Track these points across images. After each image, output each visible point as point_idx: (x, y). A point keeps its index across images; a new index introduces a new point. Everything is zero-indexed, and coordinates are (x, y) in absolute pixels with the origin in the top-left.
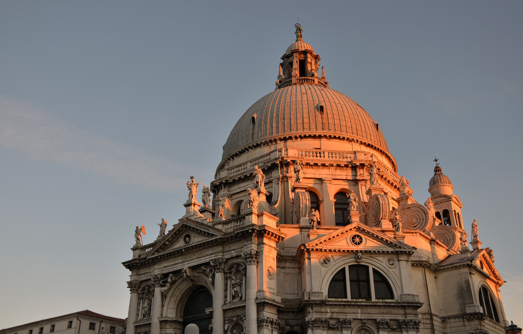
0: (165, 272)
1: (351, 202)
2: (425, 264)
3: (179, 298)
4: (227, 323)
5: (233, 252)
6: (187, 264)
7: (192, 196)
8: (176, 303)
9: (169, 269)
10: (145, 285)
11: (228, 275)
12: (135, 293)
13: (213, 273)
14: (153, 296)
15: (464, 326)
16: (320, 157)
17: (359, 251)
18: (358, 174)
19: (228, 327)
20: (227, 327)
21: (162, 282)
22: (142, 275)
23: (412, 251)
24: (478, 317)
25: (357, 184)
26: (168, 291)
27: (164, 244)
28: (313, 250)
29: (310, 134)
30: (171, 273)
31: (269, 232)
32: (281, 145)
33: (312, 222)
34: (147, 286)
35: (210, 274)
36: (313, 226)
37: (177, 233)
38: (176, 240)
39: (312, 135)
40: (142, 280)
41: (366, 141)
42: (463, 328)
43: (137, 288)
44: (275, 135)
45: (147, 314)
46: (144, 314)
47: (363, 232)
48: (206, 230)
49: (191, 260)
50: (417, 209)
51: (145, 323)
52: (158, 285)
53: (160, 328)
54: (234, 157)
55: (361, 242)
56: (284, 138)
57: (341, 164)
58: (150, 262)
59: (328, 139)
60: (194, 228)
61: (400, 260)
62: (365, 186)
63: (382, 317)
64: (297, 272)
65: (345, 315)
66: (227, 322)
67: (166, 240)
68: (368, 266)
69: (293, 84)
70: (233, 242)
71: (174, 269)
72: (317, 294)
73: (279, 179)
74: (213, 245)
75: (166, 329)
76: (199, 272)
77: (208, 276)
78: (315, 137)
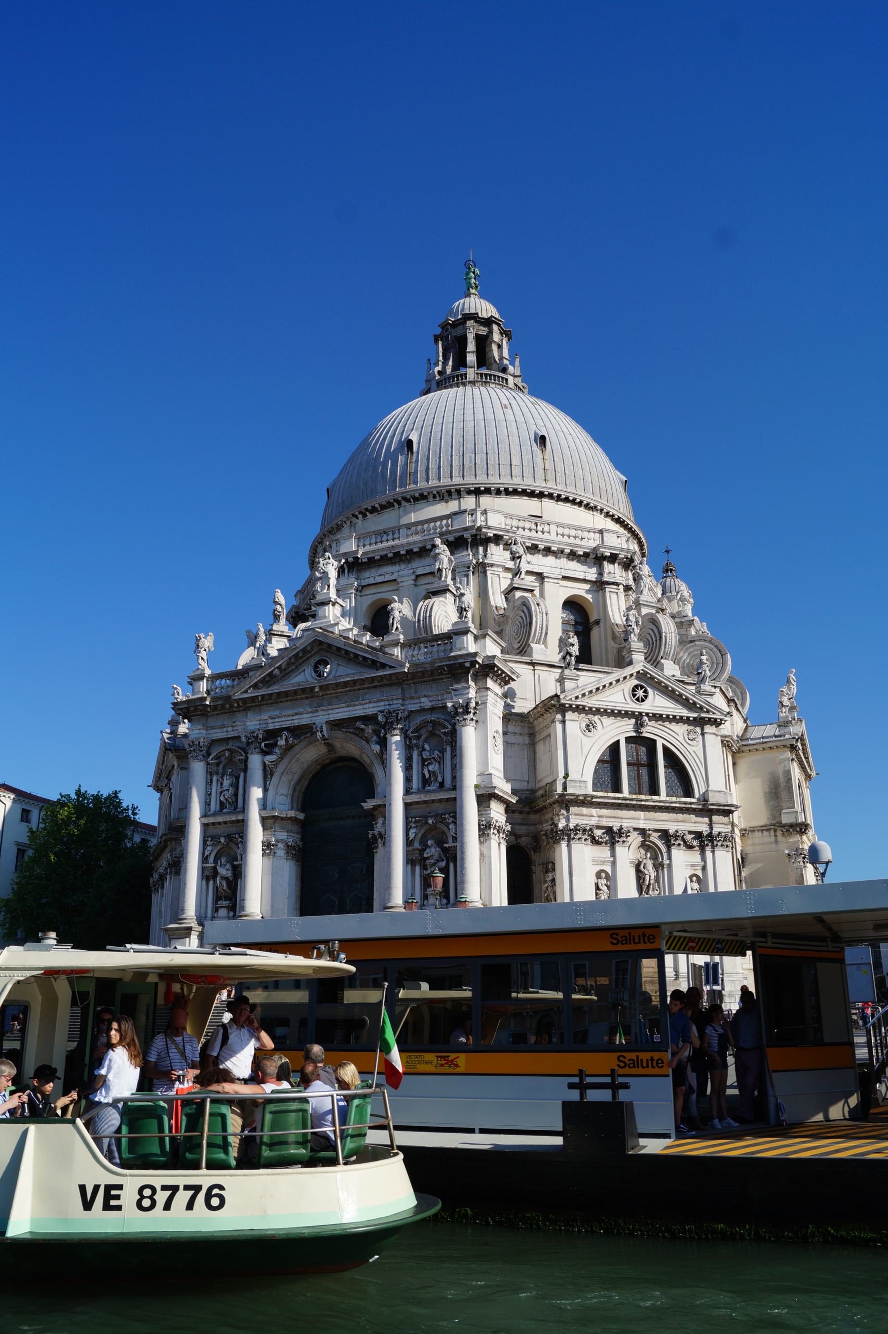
0: (271, 727)
1: (631, 626)
2: (727, 741)
3: (296, 778)
4: (414, 827)
5: (423, 700)
7: (329, 586)
9: (282, 721)
10: (225, 748)
11: (415, 742)
12: (201, 761)
13: (382, 735)
14: (245, 770)
15: (776, 842)
16: (543, 533)
17: (644, 714)
18: (606, 571)
19: (416, 834)
20: (414, 834)
22: (215, 728)
23: (726, 719)
24: (801, 829)
25: (603, 589)
26: (276, 763)
27: (271, 674)
28: (571, 705)
29: (525, 487)
30: (287, 729)
31: (499, 669)
32: (469, 502)
33: (568, 657)
34: (229, 750)
36: (569, 664)
37: (301, 655)
39: (528, 491)
41: (615, 512)
42: (774, 846)
44: (457, 480)
45: (229, 802)
46: (221, 803)
47: (650, 681)
48: (370, 654)
49: (332, 709)
50: (707, 644)
51: (229, 820)
52: (257, 750)
54: (368, 513)
55: (646, 697)
56: (475, 488)
57: (577, 551)
58: (236, 705)
59: (554, 500)
60: (339, 649)
61: (706, 733)
62: (617, 593)
63: (677, 827)
64: (527, 742)
65: (620, 820)
67: (276, 666)
68: (654, 741)
69: (470, 382)
71: (293, 722)
72: (577, 784)
73: (469, 567)
75: (275, 831)
77: (367, 741)
78: (532, 494)
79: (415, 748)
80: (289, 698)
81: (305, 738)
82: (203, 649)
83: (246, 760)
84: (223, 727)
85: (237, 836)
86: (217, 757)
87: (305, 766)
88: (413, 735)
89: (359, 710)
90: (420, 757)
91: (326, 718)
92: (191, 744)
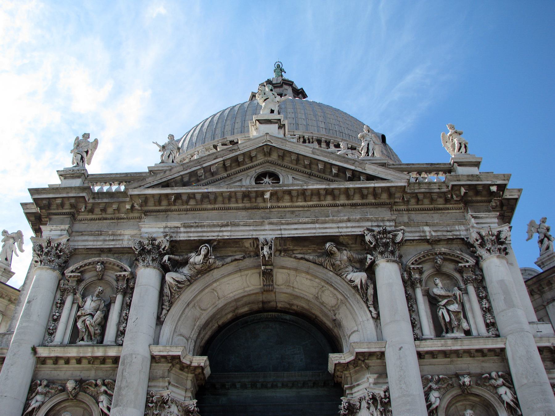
0: (182, 237)
5: (427, 229)
6: (271, 230)
8: (195, 327)
11: (417, 276)
12: (54, 269)
13: (369, 261)
21: (169, 259)
27: (193, 174)
30: (209, 242)
34: (103, 263)
35: (347, 267)
38: (225, 178)
40: (80, 247)
43: (61, 260)
45: (89, 332)
49: (288, 224)
51: (89, 355)
53: (148, 379)
66: (434, 386)
67: (204, 165)
70: (423, 210)
71: (221, 234)
74: (364, 201)
76: (302, 258)
77: (338, 271)
79: (418, 285)
80: (217, 206)
81: (232, 261)
82: (86, 150)
83: (133, 276)
84: (98, 235)
85: (99, 382)
86: (82, 271)
87: (221, 304)
88: (415, 266)
89: (331, 230)
90: (426, 297)
91: (277, 234)
92: (44, 245)
